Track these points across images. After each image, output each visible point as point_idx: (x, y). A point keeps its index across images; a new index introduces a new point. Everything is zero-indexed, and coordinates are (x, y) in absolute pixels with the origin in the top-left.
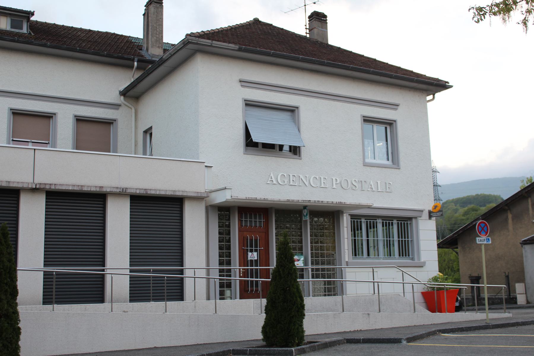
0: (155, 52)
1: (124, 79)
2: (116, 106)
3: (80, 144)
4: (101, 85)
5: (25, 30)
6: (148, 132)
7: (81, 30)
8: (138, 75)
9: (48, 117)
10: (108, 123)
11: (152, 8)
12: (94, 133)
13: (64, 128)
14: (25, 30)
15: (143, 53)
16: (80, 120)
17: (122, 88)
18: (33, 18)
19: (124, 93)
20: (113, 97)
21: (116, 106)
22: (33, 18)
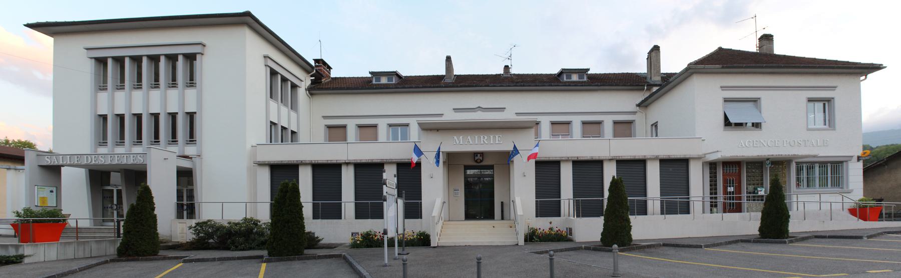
0: (657, 79)
1: (639, 97)
2: (634, 113)
3: (616, 135)
4: (624, 102)
5: (585, 79)
6: (655, 125)
7: (527, 75)
8: (647, 94)
9: (599, 123)
10: (630, 123)
11: (653, 54)
12: (624, 128)
13: (608, 128)
14: (585, 79)
15: (648, 80)
16: (615, 123)
17: (639, 101)
18: (589, 72)
19: (638, 105)
20: (632, 107)
21: (634, 113)
22: (589, 72)
